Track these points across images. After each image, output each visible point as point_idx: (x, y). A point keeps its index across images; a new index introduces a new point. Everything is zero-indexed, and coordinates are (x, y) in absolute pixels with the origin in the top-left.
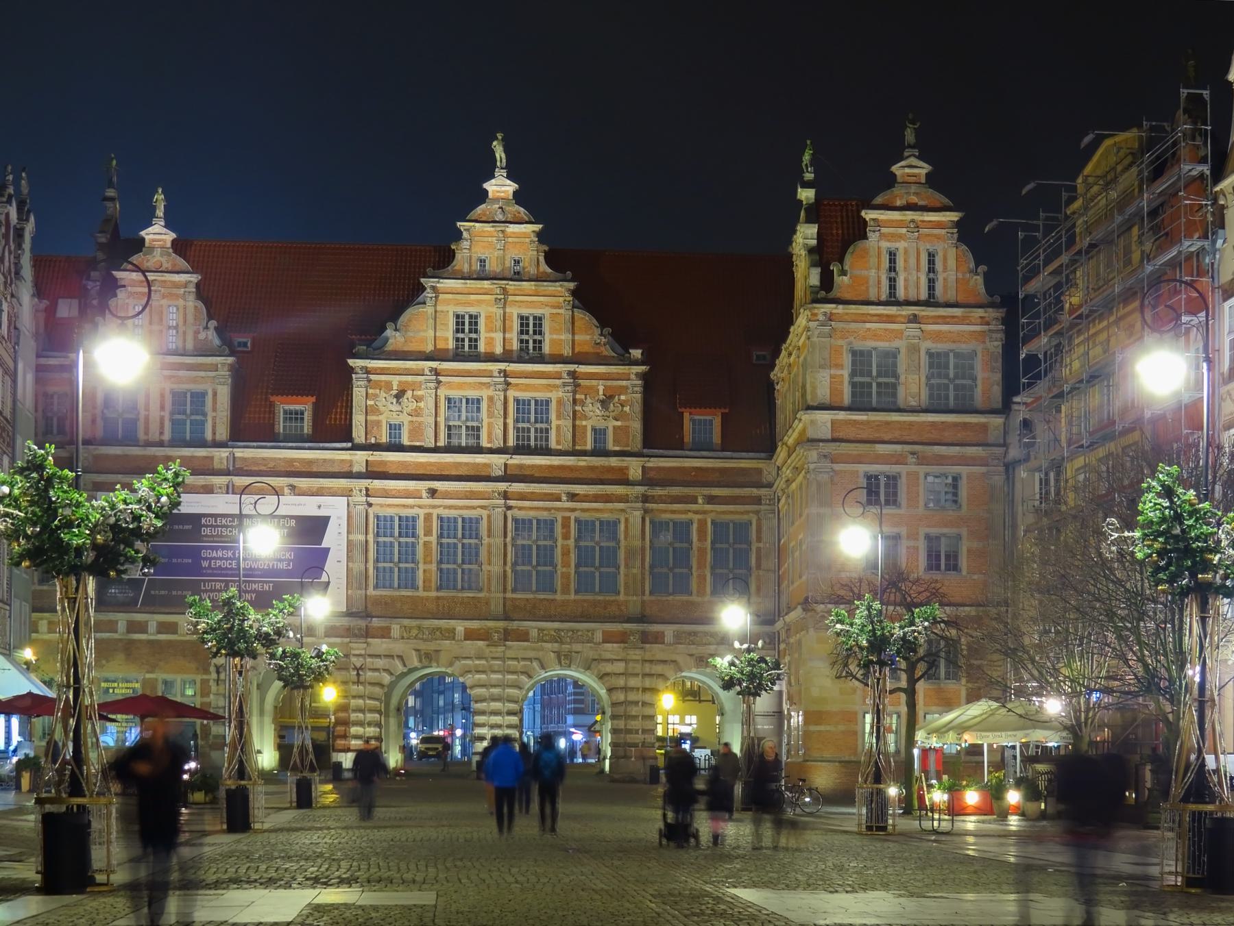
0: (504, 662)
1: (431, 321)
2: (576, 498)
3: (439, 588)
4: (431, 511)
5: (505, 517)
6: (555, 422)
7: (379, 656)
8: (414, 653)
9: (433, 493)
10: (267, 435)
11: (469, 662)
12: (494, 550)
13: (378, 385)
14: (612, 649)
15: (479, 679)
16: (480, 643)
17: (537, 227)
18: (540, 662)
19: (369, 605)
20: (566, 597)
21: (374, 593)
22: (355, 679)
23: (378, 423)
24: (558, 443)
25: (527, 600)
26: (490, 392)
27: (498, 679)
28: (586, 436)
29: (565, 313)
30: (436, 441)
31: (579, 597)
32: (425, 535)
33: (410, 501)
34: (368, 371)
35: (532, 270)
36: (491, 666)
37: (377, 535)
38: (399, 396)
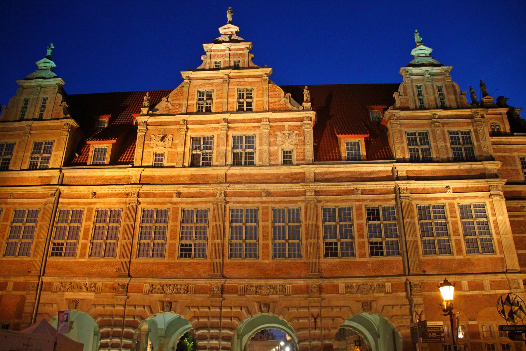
0: (221, 309)
5: (225, 207)
6: (258, 148)
9: (179, 194)
10: (83, 164)
14: (298, 299)
17: (248, 45)
18: (247, 308)
20: (267, 261)
24: (260, 160)
26: (219, 132)
28: (278, 155)
29: (265, 86)
30: (183, 162)
34: (146, 124)
35: (246, 65)
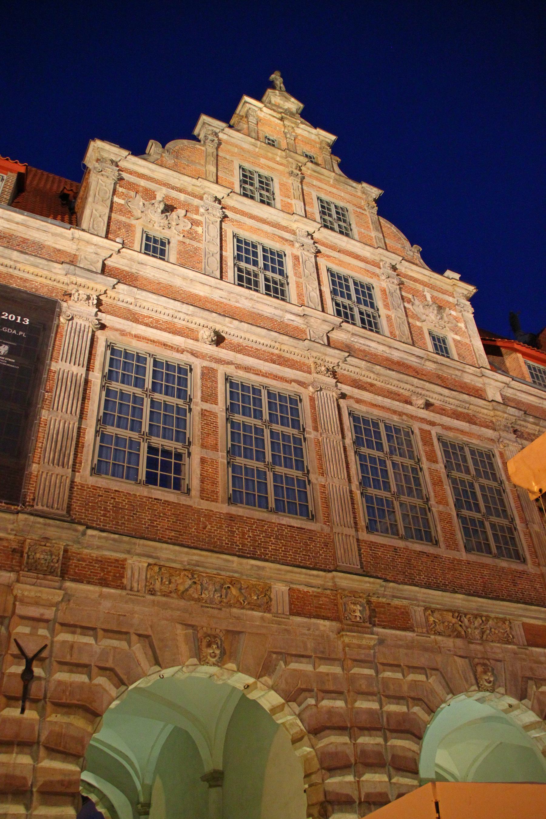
1: (212, 159)
2: (431, 408)
3: (232, 500)
4: (214, 365)
7: (86, 630)
8: (180, 631)
11: (306, 667)
12: (328, 451)
13: (131, 186)
15: (330, 712)
16: (325, 625)
19: (75, 506)
21: (92, 481)
22: (17, 687)
23: (129, 228)
25: (395, 549)
27: (370, 712)
31: (473, 557)
32: (204, 399)
33: (178, 340)
36: (352, 680)
37: (109, 376)
38: (168, 209)
